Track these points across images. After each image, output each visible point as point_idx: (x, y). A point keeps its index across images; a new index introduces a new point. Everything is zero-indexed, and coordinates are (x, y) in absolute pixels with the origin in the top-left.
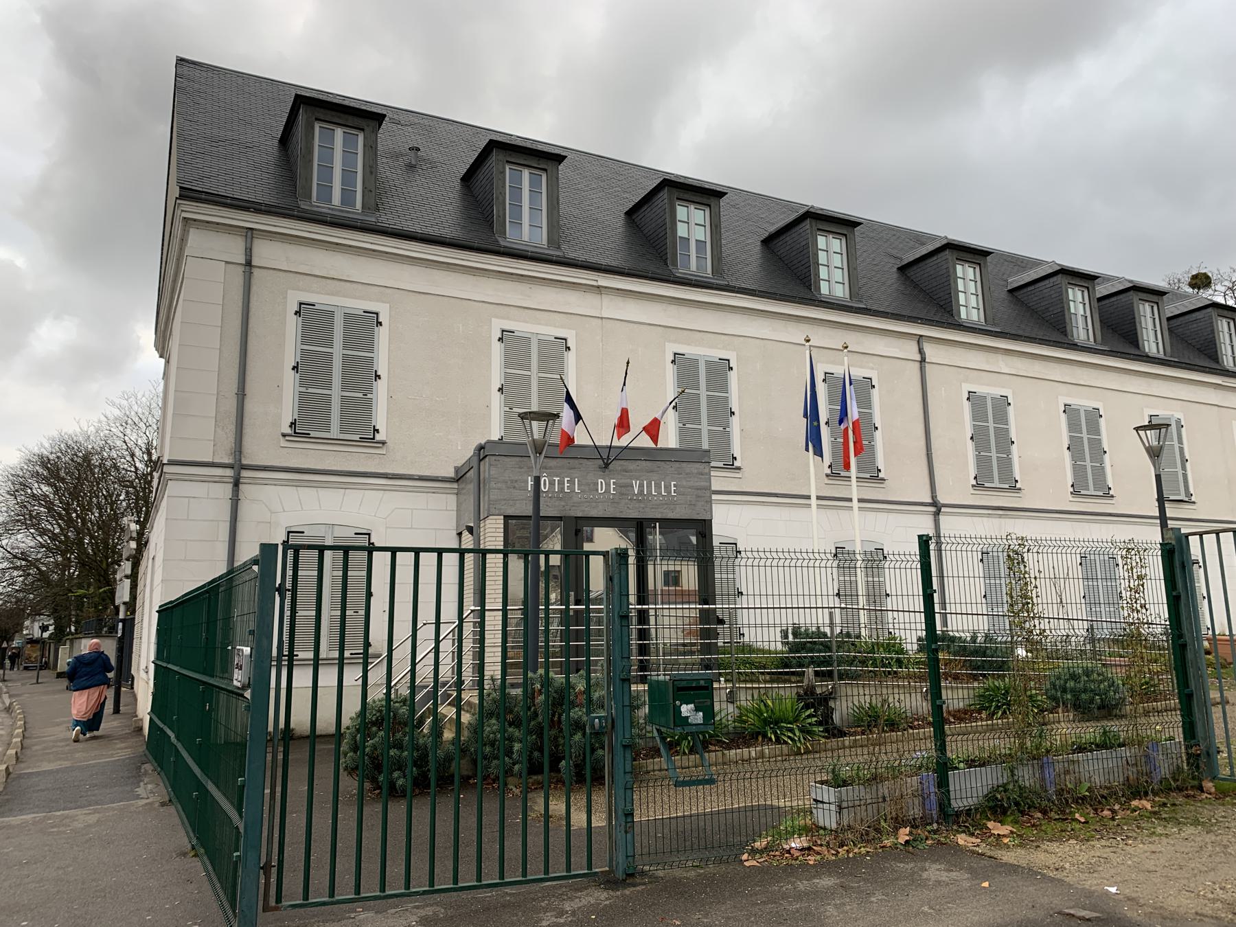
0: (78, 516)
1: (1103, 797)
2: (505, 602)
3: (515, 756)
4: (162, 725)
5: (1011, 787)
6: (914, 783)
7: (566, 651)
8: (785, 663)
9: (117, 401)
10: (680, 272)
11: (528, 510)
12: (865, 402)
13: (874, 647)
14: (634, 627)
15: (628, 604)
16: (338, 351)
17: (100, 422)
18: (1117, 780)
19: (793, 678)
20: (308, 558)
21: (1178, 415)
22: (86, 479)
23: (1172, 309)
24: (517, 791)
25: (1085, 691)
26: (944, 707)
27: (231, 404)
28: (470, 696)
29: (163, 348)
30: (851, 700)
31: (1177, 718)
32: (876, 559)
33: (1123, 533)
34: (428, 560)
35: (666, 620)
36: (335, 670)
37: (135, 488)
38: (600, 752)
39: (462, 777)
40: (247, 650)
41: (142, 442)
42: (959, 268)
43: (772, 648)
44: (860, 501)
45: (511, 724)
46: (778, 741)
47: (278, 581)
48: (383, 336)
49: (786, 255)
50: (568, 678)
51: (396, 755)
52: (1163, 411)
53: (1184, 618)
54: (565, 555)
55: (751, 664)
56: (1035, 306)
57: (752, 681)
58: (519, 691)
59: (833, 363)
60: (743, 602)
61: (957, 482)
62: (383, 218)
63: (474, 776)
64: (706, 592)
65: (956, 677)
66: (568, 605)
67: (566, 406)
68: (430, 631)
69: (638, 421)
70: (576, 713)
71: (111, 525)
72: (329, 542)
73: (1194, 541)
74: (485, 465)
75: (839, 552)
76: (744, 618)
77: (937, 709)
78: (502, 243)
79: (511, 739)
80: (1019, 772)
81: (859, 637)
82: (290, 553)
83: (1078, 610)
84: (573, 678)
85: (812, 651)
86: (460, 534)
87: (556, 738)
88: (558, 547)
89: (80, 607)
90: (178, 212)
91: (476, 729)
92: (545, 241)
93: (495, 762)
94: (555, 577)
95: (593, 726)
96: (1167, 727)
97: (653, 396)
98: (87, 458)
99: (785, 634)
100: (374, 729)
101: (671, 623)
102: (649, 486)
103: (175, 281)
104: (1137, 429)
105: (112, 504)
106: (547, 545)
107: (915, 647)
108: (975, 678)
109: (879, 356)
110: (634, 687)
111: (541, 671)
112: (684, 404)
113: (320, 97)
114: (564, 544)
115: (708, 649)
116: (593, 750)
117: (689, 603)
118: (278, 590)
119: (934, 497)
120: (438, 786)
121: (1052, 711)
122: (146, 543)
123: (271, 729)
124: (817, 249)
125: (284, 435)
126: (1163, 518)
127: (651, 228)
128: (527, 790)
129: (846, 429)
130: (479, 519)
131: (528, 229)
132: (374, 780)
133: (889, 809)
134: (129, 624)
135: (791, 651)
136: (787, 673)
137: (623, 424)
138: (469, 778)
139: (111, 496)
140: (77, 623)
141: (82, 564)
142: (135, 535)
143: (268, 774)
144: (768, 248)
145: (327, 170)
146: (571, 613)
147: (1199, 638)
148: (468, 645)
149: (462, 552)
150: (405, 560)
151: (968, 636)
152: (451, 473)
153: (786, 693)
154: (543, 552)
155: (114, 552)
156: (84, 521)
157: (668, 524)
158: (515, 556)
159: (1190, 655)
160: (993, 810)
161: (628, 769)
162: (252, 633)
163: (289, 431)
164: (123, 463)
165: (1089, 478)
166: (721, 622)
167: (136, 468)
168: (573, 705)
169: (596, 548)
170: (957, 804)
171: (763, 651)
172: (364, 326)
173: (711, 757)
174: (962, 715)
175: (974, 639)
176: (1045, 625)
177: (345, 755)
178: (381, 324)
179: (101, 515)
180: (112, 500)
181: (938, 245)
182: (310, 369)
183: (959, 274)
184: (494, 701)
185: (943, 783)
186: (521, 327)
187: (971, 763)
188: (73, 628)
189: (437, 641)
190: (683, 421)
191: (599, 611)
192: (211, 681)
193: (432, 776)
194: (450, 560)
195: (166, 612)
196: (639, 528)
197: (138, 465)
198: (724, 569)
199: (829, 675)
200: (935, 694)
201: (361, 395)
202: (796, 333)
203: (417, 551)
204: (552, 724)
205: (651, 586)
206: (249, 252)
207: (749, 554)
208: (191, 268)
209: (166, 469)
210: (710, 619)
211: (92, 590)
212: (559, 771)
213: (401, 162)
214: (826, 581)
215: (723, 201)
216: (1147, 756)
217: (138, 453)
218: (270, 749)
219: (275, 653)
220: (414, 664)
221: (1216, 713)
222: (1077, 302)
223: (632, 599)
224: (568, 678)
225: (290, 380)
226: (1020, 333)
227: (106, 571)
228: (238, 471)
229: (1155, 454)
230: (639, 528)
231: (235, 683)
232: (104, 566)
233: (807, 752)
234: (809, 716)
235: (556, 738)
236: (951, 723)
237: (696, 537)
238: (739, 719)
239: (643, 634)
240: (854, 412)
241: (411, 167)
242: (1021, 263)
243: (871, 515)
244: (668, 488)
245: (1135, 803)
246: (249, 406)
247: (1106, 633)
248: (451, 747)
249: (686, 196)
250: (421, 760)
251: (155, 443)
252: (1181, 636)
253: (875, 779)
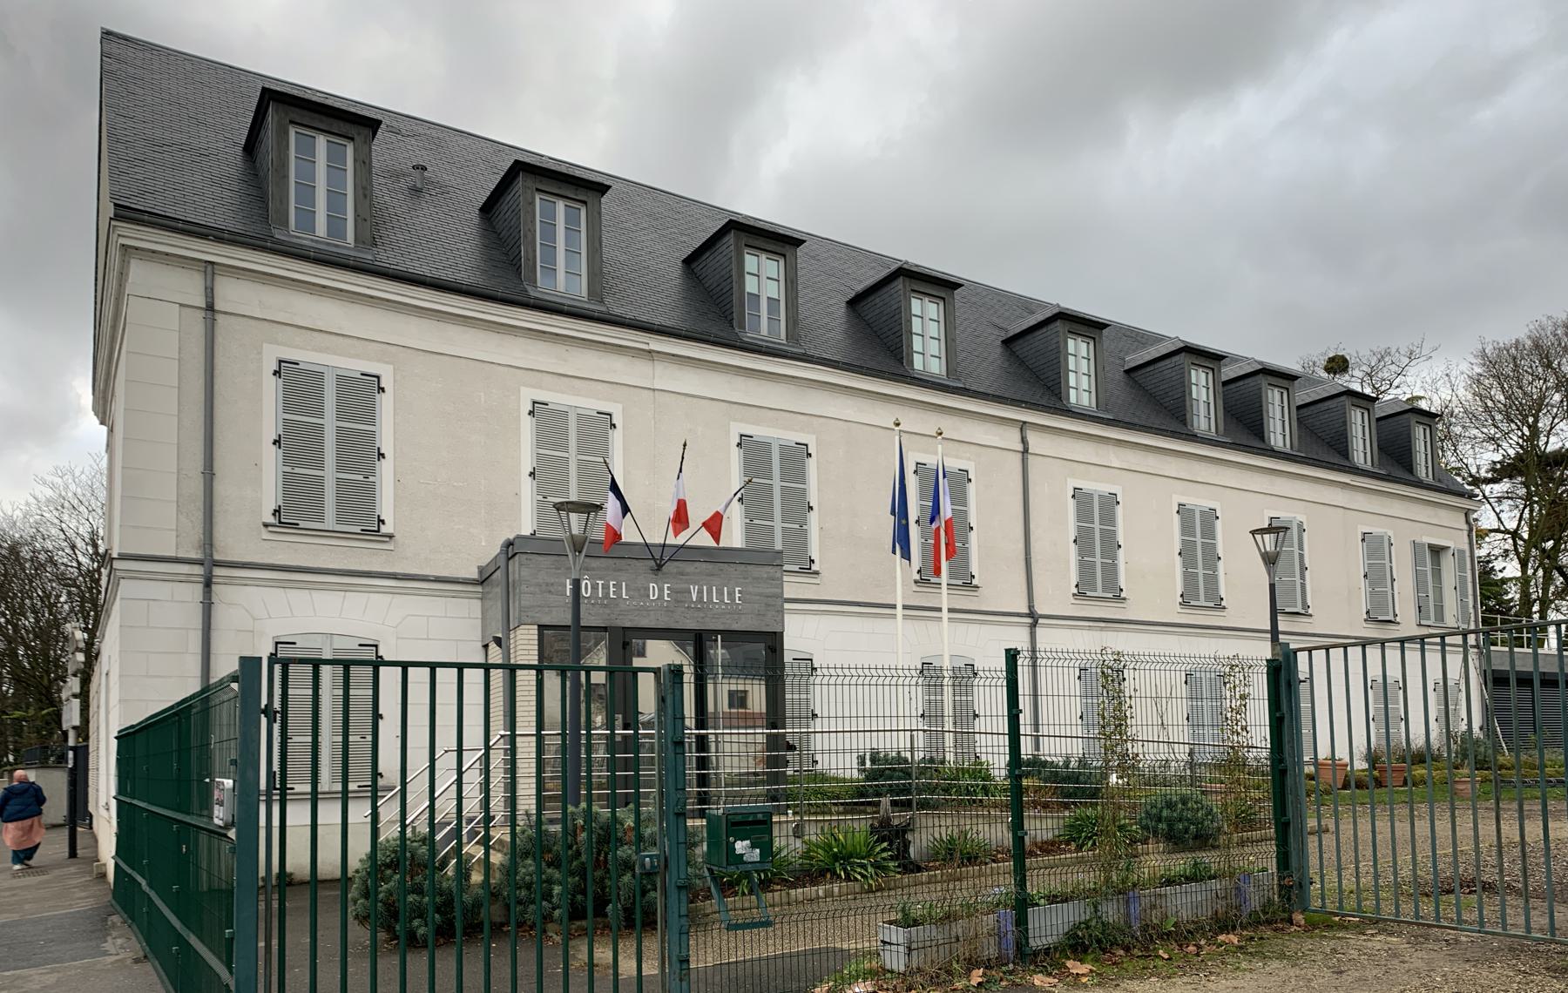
0: (8, 622)
1: (1189, 932)
2: (540, 725)
3: (554, 900)
4: (129, 871)
5: (1093, 923)
6: (991, 922)
7: (613, 782)
8: (861, 792)
9: (49, 478)
10: (749, 336)
11: (566, 618)
12: (960, 498)
13: (960, 772)
14: (692, 755)
15: (684, 727)
16: (330, 422)
17: (27, 504)
18: (1205, 914)
19: (869, 809)
20: (301, 674)
21: (1301, 518)
22: (15, 575)
23: (1303, 396)
24: (558, 939)
25: (1180, 820)
26: (1027, 839)
27: (196, 486)
28: (500, 834)
29: (104, 413)
30: (929, 832)
31: (1272, 848)
32: (966, 675)
33: (1227, 648)
34: (447, 677)
35: (727, 747)
36: (338, 806)
37: (78, 587)
38: (652, 894)
39: (493, 924)
40: (229, 783)
41: (84, 530)
42: (1071, 343)
43: (848, 776)
44: (950, 610)
45: (549, 865)
46: (848, 879)
47: (264, 702)
48: (386, 405)
49: (875, 319)
50: (614, 813)
51: (411, 897)
52: (1284, 513)
53: (1286, 738)
54: (610, 672)
55: (824, 794)
56: (1155, 390)
57: (823, 813)
58: (558, 828)
59: (926, 452)
60: (818, 725)
61: (1056, 594)
62: (382, 256)
63: (508, 924)
64: (775, 714)
65: (1046, 806)
66: (613, 731)
67: (611, 495)
68: (452, 756)
69: (697, 516)
70: (624, 852)
71: (51, 633)
72: (327, 655)
73: (1302, 658)
74: (514, 565)
75: (926, 669)
76: (818, 742)
77: (1019, 841)
78: (532, 293)
79: (550, 881)
80: (1103, 908)
81: (943, 762)
82: (277, 668)
83: (1181, 733)
84: (621, 812)
85: (891, 778)
86: (486, 647)
87: (602, 879)
88: (603, 663)
89: (18, 732)
90: (114, 237)
91: (510, 870)
92: (584, 293)
93: (532, 907)
94: (600, 697)
95: (643, 865)
96: (1261, 858)
97: (716, 485)
98: (14, 549)
99: (862, 761)
100: (389, 872)
101: (736, 752)
102: (710, 592)
103: (114, 327)
104: (1253, 533)
105: (51, 606)
106: (589, 661)
107: (1003, 773)
108: (1066, 806)
109: (976, 445)
110: (690, 823)
111: (583, 805)
112: (752, 495)
113: (295, 92)
114: (610, 659)
115: (775, 778)
116: (644, 893)
117: (754, 727)
118: (265, 712)
119: (1031, 607)
120: (465, 934)
121: (1145, 841)
122: (98, 654)
123: (262, 873)
124: (911, 315)
125: (266, 525)
126: (1274, 632)
127: (713, 281)
128: (569, 937)
129: (938, 529)
130: (508, 629)
131: (564, 276)
132: (390, 929)
133: (962, 950)
134: (82, 753)
135: (867, 779)
136: (862, 804)
137: (680, 518)
138: (502, 925)
139: (49, 597)
140: (16, 751)
141: (17, 680)
142: (82, 645)
143: (262, 925)
144: (854, 310)
145: (307, 191)
146: (618, 739)
147: (1301, 763)
148: (498, 778)
149: (487, 668)
150: (419, 676)
151: (1060, 761)
153: (858, 827)
154: (584, 668)
155: (57, 666)
156: (15, 627)
157: (732, 637)
158: (553, 673)
159: (1289, 780)
160: (1074, 948)
161: (684, 911)
162: (233, 762)
163: (271, 520)
164: (62, 558)
165: (1201, 590)
166: (791, 748)
167: (79, 564)
168: (621, 842)
169: (645, 665)
170: (1035, 943)
171: (837, 780)
172: (362, 392)
173: (776, 896)
174: (1048, 847)
175: (1067, 764)
176: (1138, 748)
177: (355, 902)
178: (383, 390)
179: (37, 621)
180: (49, 602)
181: (1048, 314)
182: (296, 444)
183: (1071, 349)
184: (530, 839)
185: (1021, 922)
186: (556, 397)
187: (1053, 899)
188: (11, 758)
189: (460, 773)
190: (750, 516)
191: (651, 736)
192: (187, 819)
193: (458, 925)
194: (474, 677)
195: (127, 738)
196: (698, 642)
197: (81, 558)
198: (796, 689)
199: (907, 805)
200: (1017, 826)
202: (883, 415)
203: (433, 667)
204: (597, 865)
205: (711, 708)
206: (210, 292)
207: (825, 671)
208: (134, 310)
209: (116, 565)
210: (779, 748)
211: (31, 712)
212: (606, 915)
213: (403, 184)
214: (911, 701)
215: (801, 251)
216: (1238, 889)
217: (80, 544)
218: (262, 897)
219: (263, 785)
220: (432, 799)
221: (1312, 843)
222: (1200, 386)
223: (690, 721)
224: (614, 813)
225: (271, 458)
226: (1136, 420)
227: (48, 689)
228: (210, 569)
229: (1270, 560)
230: (698, 642)
231: (216, 821)
232: (46, 682)
233: (879, 889)
234: (884, 850)
235: (602, 879)
236: (1037, 856)
237: (764, 652)
238: (806, 855)
239: (703, 763)
240: (947, 510)
241: (416, 191)
242: (1140, 338)
243: (963, 627)
244: (731, 594)
245: (1222, 938)
246: (220, 488)
247: (1208, 758)
248: (481, 891)
249: (757, 243)
250: (446, 907)
251: (101, 533)
252: (1281, 761)
253: (949, 917)
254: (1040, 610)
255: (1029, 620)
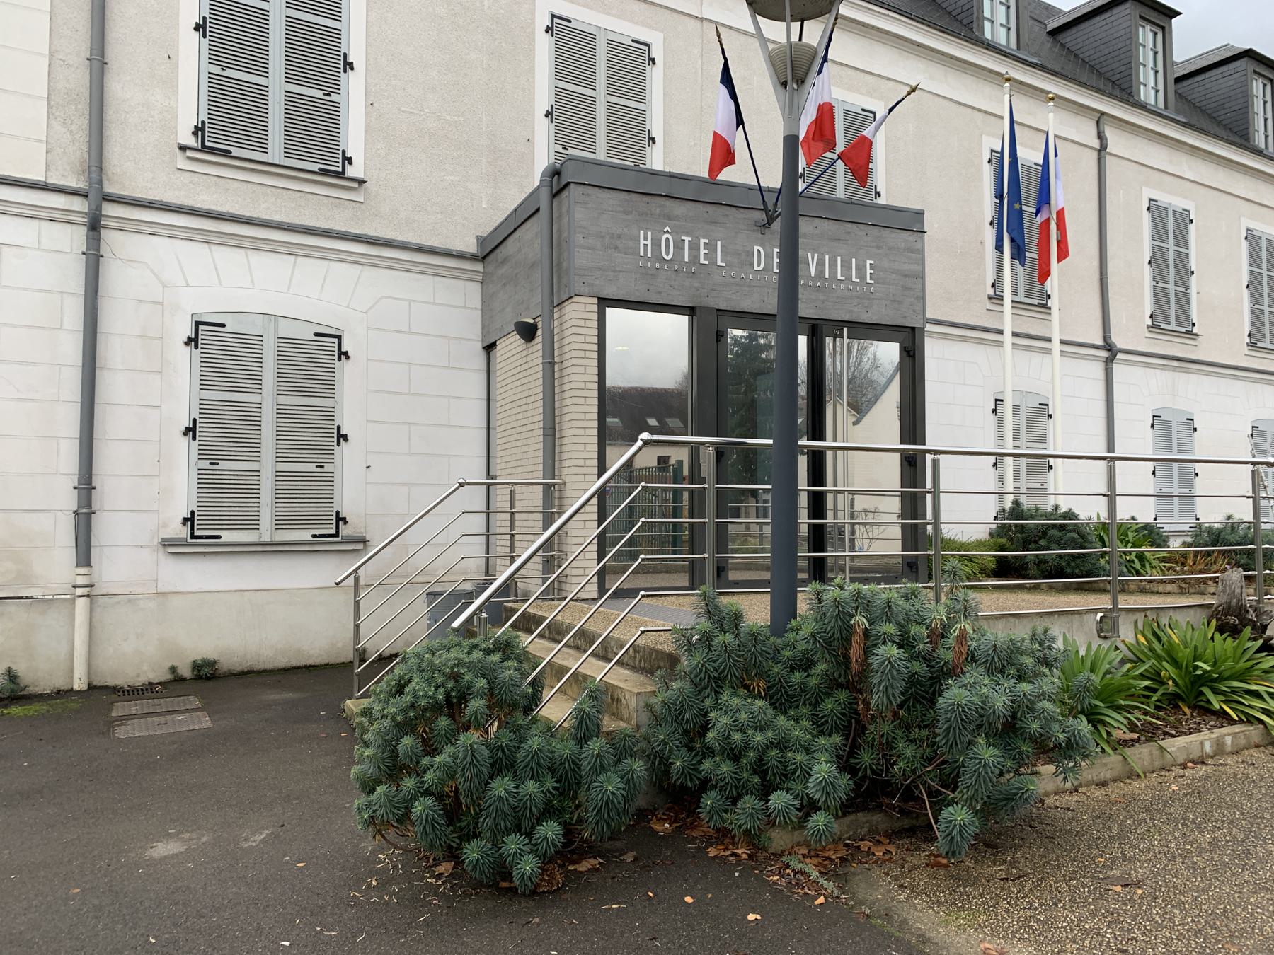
27: (77, 78)
125: (183, 148)
129: (1047, 222)
152: (471, 247)
163: (191, 141)
201: (319, 94)
225: (191, 52)
246: (117, 87)
254: (1119, 341)
255: (1104, 354)
